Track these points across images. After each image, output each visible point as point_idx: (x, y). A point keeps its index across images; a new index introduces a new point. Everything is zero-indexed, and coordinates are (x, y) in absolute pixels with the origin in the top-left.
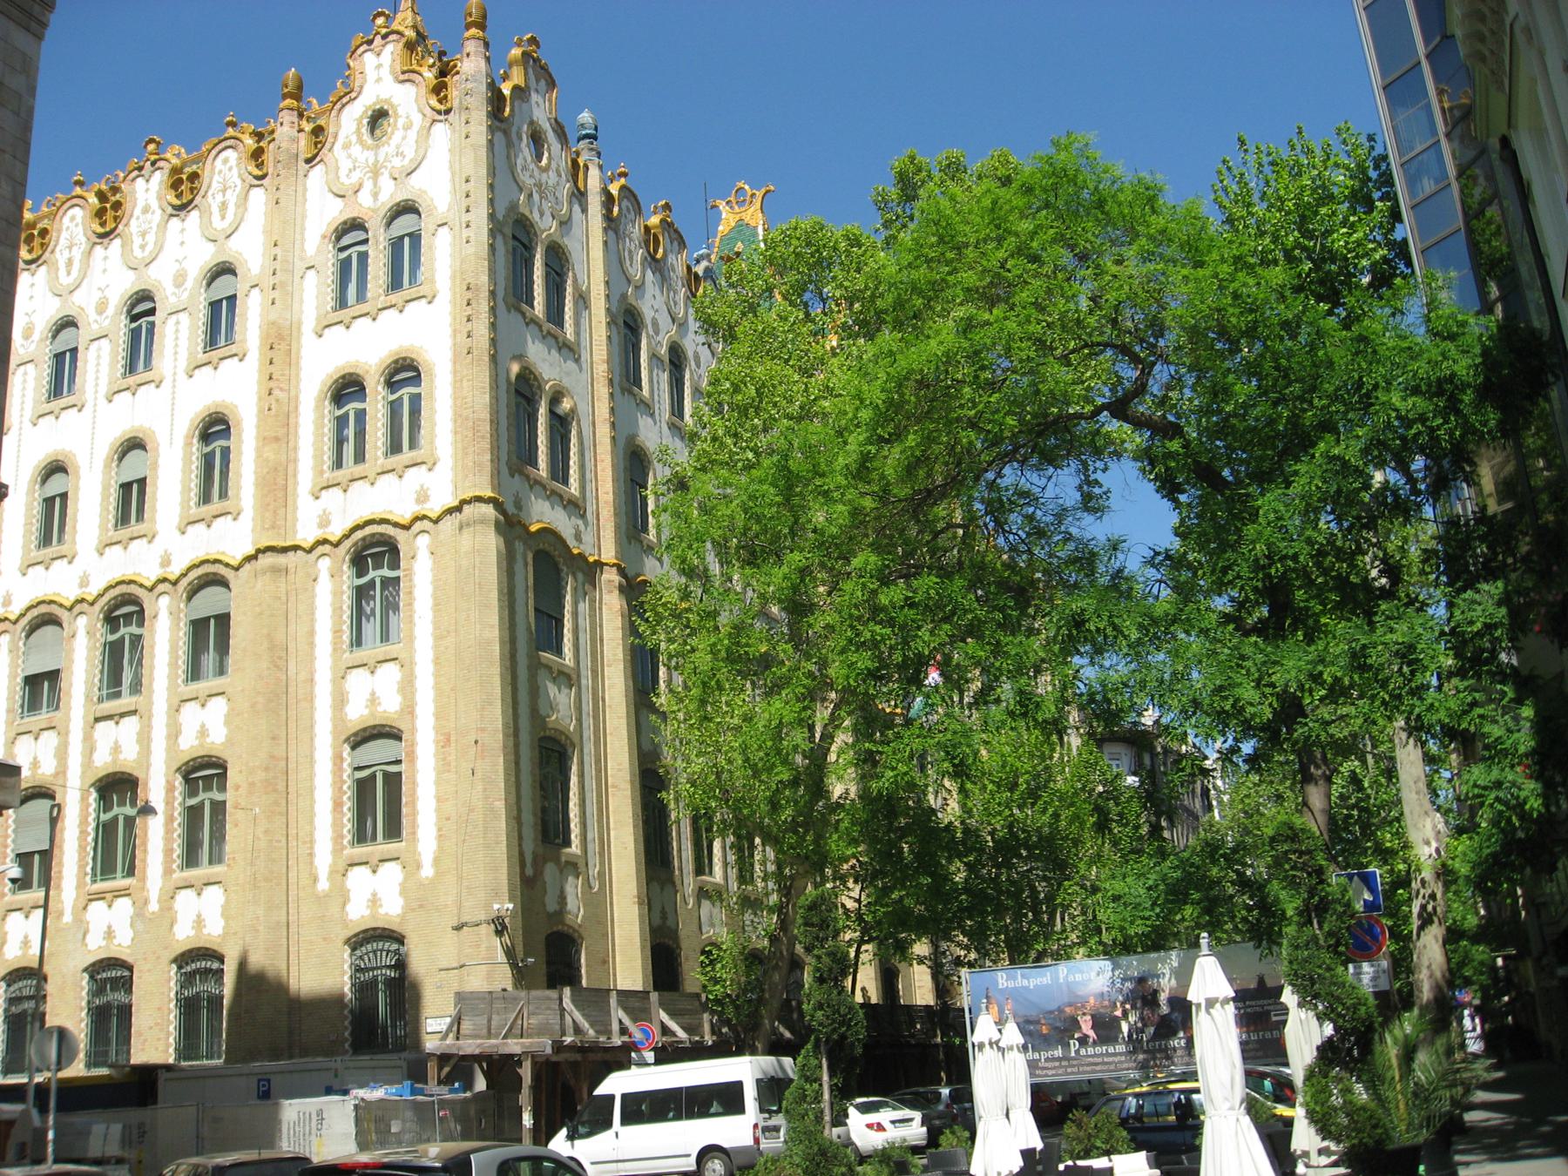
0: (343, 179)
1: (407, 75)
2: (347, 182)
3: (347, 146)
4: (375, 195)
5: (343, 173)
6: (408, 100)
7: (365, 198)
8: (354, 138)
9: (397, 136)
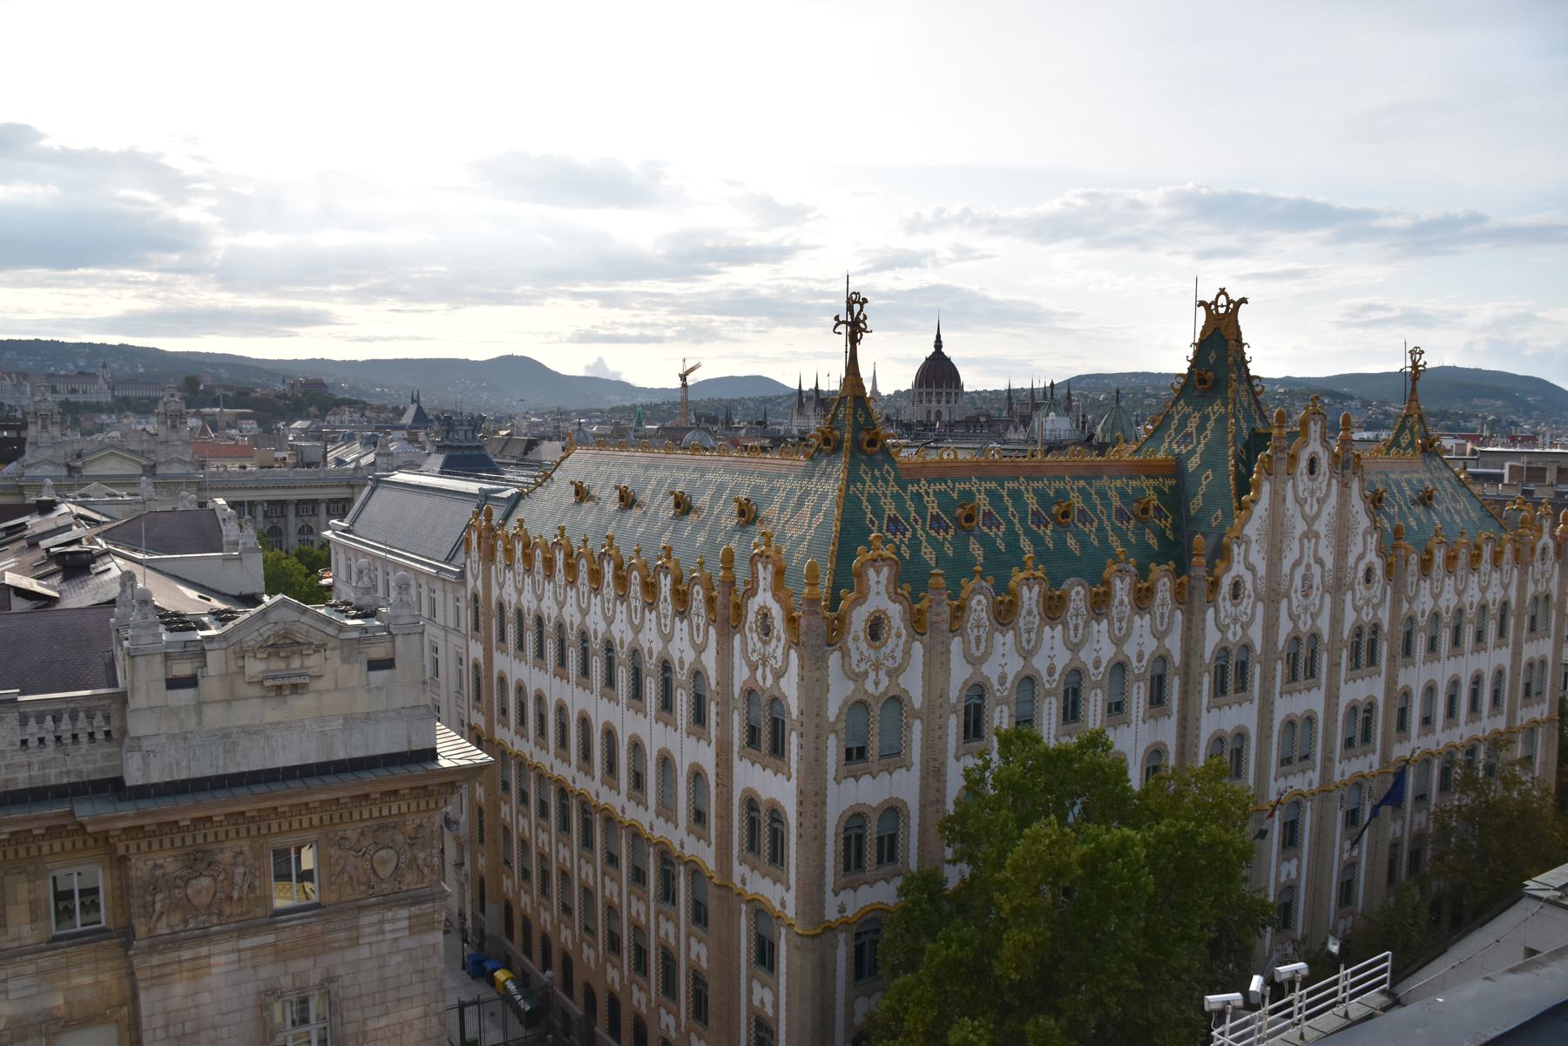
0: (854, 666)
1: (895, 597)
3: (856, 639)
4: (877, 684)
5: (854, 662)
6: (895, 611)
7: (869, 686)
8: (862, 635)
9: (891, 643)
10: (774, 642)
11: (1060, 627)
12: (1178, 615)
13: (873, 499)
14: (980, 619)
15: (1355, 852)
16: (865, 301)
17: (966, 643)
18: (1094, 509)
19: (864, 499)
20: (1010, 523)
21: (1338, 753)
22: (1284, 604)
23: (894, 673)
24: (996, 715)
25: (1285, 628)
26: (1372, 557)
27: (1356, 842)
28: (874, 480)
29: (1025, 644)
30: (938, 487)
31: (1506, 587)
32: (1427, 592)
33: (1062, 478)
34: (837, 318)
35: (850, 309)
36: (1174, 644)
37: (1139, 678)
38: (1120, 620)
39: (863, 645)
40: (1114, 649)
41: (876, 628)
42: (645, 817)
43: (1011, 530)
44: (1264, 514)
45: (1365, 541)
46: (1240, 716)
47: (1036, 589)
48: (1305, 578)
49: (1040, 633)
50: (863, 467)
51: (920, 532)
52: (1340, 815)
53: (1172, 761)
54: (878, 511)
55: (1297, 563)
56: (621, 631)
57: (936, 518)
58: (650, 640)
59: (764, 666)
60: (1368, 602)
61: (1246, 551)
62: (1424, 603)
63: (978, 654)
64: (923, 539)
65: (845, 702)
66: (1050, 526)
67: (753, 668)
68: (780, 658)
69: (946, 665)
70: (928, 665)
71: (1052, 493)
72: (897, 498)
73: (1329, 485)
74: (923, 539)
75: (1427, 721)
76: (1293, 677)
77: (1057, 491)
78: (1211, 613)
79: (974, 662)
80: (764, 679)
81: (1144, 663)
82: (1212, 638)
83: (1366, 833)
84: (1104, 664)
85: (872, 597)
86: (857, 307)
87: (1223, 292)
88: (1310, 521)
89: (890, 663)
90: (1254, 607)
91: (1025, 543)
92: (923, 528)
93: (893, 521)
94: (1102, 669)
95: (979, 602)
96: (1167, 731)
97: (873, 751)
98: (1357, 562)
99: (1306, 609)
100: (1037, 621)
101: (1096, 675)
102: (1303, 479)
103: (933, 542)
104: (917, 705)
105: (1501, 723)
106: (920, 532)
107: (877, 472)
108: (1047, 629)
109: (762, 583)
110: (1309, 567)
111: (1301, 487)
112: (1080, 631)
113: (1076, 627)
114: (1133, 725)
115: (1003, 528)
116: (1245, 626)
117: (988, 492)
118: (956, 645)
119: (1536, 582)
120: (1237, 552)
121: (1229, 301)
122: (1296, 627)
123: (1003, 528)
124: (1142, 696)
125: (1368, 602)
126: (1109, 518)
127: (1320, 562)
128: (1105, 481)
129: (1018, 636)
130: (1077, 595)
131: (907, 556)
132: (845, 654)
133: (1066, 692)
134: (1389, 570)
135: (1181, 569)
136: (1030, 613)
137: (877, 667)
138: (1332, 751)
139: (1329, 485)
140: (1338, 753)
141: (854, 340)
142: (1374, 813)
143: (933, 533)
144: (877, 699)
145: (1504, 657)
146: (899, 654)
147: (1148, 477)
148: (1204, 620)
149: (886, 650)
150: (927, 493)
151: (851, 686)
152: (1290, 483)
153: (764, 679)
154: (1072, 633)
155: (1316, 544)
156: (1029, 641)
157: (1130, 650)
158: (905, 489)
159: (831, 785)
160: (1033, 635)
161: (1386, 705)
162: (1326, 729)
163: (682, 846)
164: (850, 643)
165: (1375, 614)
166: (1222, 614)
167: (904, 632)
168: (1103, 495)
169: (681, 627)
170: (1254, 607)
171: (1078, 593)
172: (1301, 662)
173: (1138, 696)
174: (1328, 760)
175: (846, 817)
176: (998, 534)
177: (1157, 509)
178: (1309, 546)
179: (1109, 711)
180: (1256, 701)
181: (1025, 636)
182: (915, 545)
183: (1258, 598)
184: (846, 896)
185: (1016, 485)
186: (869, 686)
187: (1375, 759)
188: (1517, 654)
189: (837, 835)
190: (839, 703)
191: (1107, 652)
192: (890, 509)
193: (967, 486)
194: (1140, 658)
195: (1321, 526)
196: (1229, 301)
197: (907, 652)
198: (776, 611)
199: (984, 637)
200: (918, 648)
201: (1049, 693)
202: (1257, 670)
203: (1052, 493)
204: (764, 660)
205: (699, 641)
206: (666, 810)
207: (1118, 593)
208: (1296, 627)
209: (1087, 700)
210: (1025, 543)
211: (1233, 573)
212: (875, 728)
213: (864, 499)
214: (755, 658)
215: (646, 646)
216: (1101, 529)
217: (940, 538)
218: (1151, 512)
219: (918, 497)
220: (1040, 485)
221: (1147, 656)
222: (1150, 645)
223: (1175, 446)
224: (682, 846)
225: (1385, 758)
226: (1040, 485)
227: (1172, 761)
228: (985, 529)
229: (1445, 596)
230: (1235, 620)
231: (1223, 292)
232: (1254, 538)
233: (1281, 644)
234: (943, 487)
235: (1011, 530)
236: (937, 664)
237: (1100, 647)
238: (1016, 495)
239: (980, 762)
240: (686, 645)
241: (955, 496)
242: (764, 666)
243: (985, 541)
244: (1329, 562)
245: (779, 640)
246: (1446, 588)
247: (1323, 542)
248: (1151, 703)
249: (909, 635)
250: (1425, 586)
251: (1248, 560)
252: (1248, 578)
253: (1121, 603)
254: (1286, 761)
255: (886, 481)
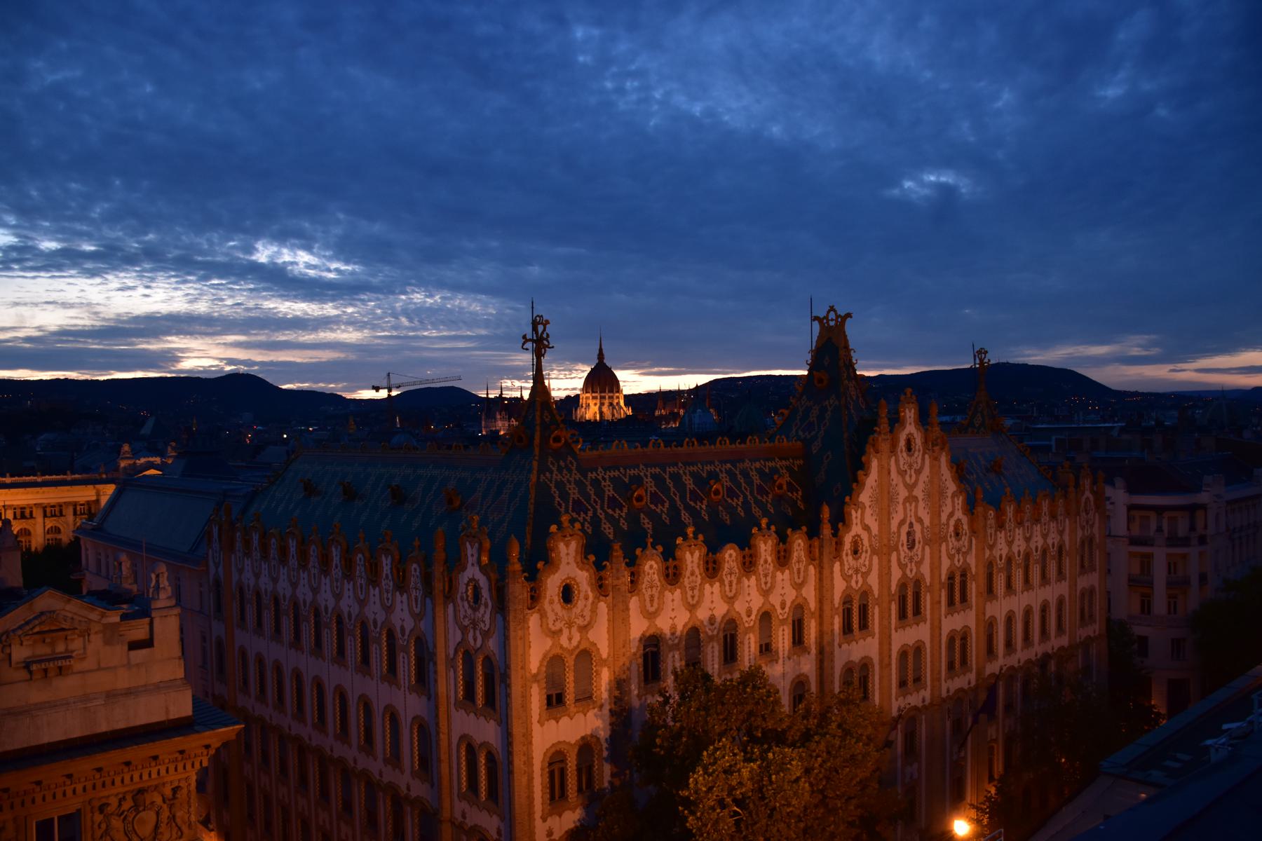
0: (551, 626)
2: (553, 628)
3: (551, 602)
4: (570, 639)
5: (551, 623)
6: (583, 578)
7: (564, 641)
8: (556, 599)
9: (580, 604)
10: (482, 609)
11: (717, 584)
12: (811, 568)
13: (560, 485)
14: (653, 581)
15: (962, 754)
16: (547, 322)
17: (642, 602)
18: (739, 486)
19: (552, 485)
20: (672, 502)
21: (943, 673)
22: (894, 555)
23: (584, 629)
24: (670, 661)
25: (896, 574)
26: (959, 514)
27: (963, 745)
28: (560, 470)
29: (690, 599)
30: (612, 474)
31: (1061, 533)
32: (1003, 541)
33: (712, 463)
34: (524, 337)
35: (535, 329)
36: (810, 593)
37: (783, 622)
38: (766, 576)
39: (557, 607)
40: (762, 600)
41: (567, 594)
42: (376, 766)
43: (673, 507)
44: (874, 484)
45: (953, 502)
46: (865, 648)
47: (697, 554)
48: (909, 534)
49: (701, 590)
50: (550, 459)
51: (599, 511)
52: (948, 724)
53: (814, 688)
54: (564, 496)
55: (902, 523)
56: (348, 604)
57: (612, 500)
58: (374, 611)
59: (475, 629)
60: (958, 551)
61: (862, 515)
62: (1002, 549)
63: (652, 610)
64: (602, 517)
65: (545, 656)
66: (705, 502)
67: (464, 630)
68: (488, 622)
69: (626, 621)
70: (612, 621)
71: (704, 475)
72: (579, 484)
73: (923, 459)
74: (602, 517)
75: (1009, 644)
76: (902, 615)
77: (710, 473)
78: (837, 566)
79: (651, 616)
80: (475, 640)
81: (787, 609)
82: (839, 586)
83: (969, 738)
84: (788, 604)
85: (563, 566)
86: (540, 328)
87: (832, 309)
88: (910, 487)
89: (580, 622)
90: (871, 561)
91: (685, 516)
92: (602, 508)
93: (577, 503)
94: (753, 617)
95: (651, 567)
96: (808, 666)
97: (570, 697)
98: (948, 519)
99: (911, 559)
100: (699, 580)
101: (750, 621)
102: (903, 456)
103: (610, 519)
104: (605, 656)
105: (1064, 641)
106: (599, 511)
107: (562, 463)
108: (707, 586)
109: (470, 559)
110: (911, 525)
111: (901, 462)
112: (734, 586)
113: (731, 582)
114: (781, 661)
115: (667, 505)
116: (865, 575)
117: (654, 476)
118: (634, 602)
119: (1083, 528)
120: (855, 515)
121: (838, 316)
122: (904, 574)
123: (667, 505)
124: (786, 637)
125: (958, 551)
126: (752, 493)
127: (920, 520)
128: (747, 464)
129: (684, 593)
130: (730, 555)
131: (590, 531)
132: (543, 615)
133: (725, 637)
134: (971, 523)
135: (814, 533)
136: (692, 574)
137: (570, 625)
138: (940, 672)
139: (923, 459)
140: (943, 673)
141: (539, 354)
142: (975, 721)
143: (610, 511)
144: (571, 652)
145: (1063, 588)
146: (587, 613)
147: (781, 459)
148: (832, 572)
149: (577, 610)
150: (604, 479)
151: (549, 642)
152: (893, 459)
153: (475, 640)
154: (727, 588)
155: (916, 507)
156: (693, 597)
157: (775, 600)
158: (585, 476)
159: (536, 728)
160: (696, 592)
161: (977, 633)
162: (932, 656)
163: (408, 789)
164: (547, 606)
165: (965, 561)
166: (846, 567)
167: (591, 595)
168: (746, 474)
169: (401, 601)
170: (871, 561)
171: (731, 556)
172: (909, 603)
173: (782, 639)
174: (936, 680)
175: (549, 755)
176: (663, 509)
177: (789, 484)
178: (911, 507)
179: (761, 651)
180: (877, 636)
181: (690, 593)
182: (596, 522)
183: (874, 552)
184: (554, 822)
185: (676, 470)
186: (564, 641)
187: (972, 676)
188: (1073, 586)
189: (542, 769)
190: (540, 656)
191: (757, 602)
192: (574, 493)
193: (636, 472)
194: (783, 606)
195: (918, 492)
196: (838, 316)
197: (594, 611)
198: (483, 581)
199: (656, 595)
200: (603, 607)
201: (711, 638)
202: (877, 610)
203: (704, 475)
204: (474, 624)
205: (417, 611)
206: (395, 759)
207: (763, 553)
208: (904, 574)
209: (742, 643)
210: (685, 516)
211: (853, 533)
212: (570, 678)
213: (552, 485)
214: (466, 622)
215: (371, 617)
216: (746, 503)
217: (616, 516)
218: (785, 487)
219: (596, 483)
220: (695, 468)
221: (788, 604)
222: (790, 595)
223: (800, 433)
224: (408, 789)
225: (979, 674)
226: (695, 468)
227: (814, 688)
228: (653, 507)
229: (1016, 542)
230: (857, 571)
231: (832, 309)
232: (867, 504)
233: (894, 588)
234: (617, 473)
235: (673, 507)
236: (619, 618)
237: (750, 600)
238: (676, 478)
239: (661, 699)
240: (406, 615)
241: (626, 480)
242: (475, 629)
243: (653, 516)
244: (927, 522)
245: (486, 606)
246: (1017, 537)
247: (921, 504)
248: (794, 643)
249: (595, 598)
250: (1001, 536)
251: (864, 520)
252: (865, 536)
253: (766, 561)
254: (902, 684)
255: (570, 471)
